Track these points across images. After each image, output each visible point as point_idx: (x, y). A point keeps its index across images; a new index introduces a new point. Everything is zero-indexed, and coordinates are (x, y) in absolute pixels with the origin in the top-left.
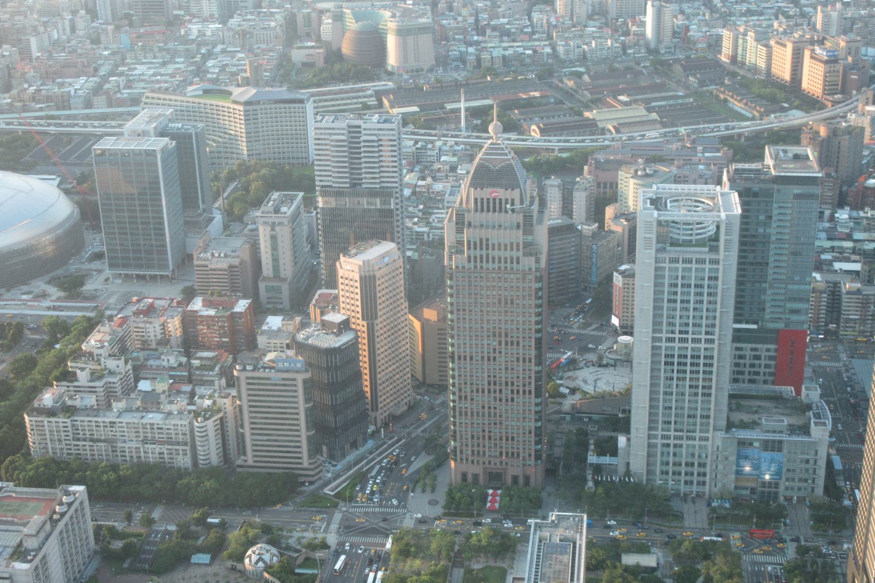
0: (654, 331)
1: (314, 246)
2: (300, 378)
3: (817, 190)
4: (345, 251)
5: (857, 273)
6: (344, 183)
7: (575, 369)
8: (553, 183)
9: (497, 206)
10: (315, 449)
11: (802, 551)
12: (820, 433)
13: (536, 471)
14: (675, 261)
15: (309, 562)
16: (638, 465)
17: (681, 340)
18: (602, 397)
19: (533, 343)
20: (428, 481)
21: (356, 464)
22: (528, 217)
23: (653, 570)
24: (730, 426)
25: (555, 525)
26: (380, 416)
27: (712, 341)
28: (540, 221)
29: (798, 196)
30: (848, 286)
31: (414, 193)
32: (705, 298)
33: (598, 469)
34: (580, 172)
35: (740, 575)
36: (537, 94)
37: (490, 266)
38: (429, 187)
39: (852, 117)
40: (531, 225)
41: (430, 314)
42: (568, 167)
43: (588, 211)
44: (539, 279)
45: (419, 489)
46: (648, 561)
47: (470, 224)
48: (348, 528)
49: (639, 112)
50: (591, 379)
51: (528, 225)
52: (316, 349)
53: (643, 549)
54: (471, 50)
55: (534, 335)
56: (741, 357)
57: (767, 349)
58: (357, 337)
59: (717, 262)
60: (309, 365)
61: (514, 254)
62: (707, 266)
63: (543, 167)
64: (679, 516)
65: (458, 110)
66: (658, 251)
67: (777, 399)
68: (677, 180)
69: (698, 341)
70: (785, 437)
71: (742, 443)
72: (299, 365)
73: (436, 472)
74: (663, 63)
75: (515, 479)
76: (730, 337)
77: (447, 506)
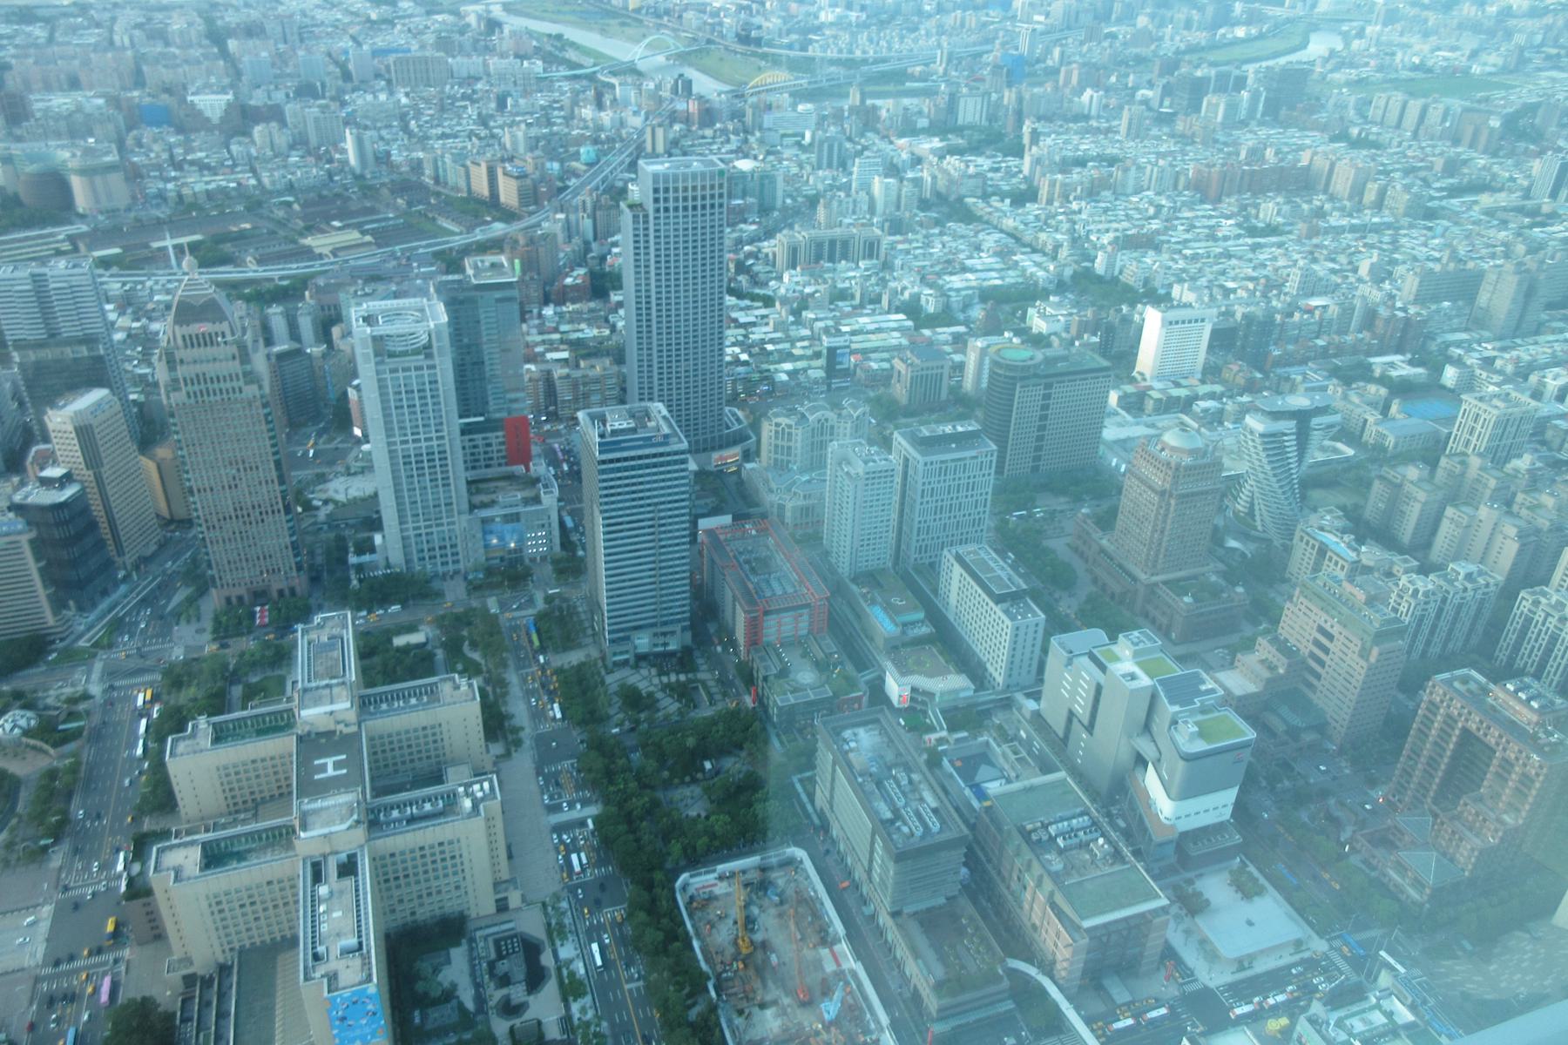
0: (388, 436)
1: (21, 404)
2: (24, 539)
3: (515, 293)
4: (52, 404)
5: (566, 360)
6: (41, 334)
7: (325, 481)
8: (275, 311)
9: (208, 340)
10: (58, 605)
11: (549, 599)
12: (550, 500)
13: (300, 582)
14: (392, 371)
15: (72, 716)
16: (397, 558)
17: (414, 441)
18: (354, 502)
19: (272, 466)
20: (191, 612)
21: (110, 610)
22: (242, 347)
23: (424, 645)
24: (473, 507)
25: (320, 627)
26: (129, 559)
27: (442, 438)
28: (256, 350)
29: (498, 300)
30: (559, 372)
31: (129, 336)
32: (429, 400)
33: (360, 568)
34: (302, 297)
35: (499, 632)
36: (248, 226)
37: (212, 398)
38: (144, 328)
39: (545, 225)
40: (247, 355)
41: (163, 452)
42: (288, 294)
43: (316, 333)
44: (265, 406)
45: (183, 622)
46: (416, 638)
47: (182, 361)
48: (111, 673)
49: (353, 236)
50: (341, 488)
51: (244, 355)
52: (42, 509)
53: (412, 629)
54: (170, 186)
55: (271, 458)
56: (475, 447)
57: (497, 437)
58: (83, 489)
59: (434, 367)
60: (29, 523)
61: (235, 384)
62: (426, 372)
63: (263, 296)
64: (440, 594)
65: (165, 248)
66: (377, 364)
67: (510, 478)
68: (396, 295)
69: (430, 439)
70: (521, 509)
71: (484, 521)
72: (20, 527)
73: (200, 602)
74: (370, 188)
75: (281, 593)
76: (458, 432)
77: (215, 631)
